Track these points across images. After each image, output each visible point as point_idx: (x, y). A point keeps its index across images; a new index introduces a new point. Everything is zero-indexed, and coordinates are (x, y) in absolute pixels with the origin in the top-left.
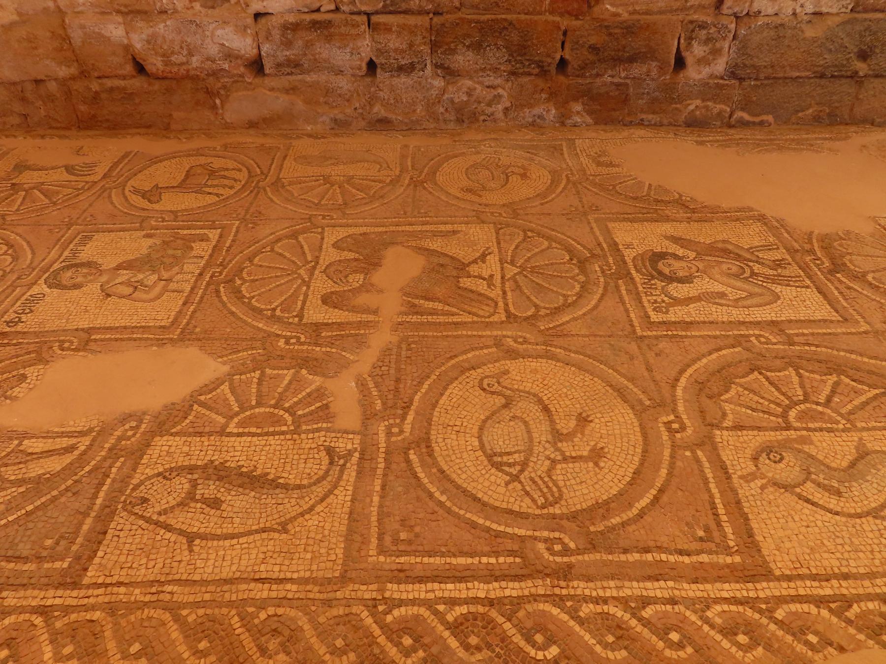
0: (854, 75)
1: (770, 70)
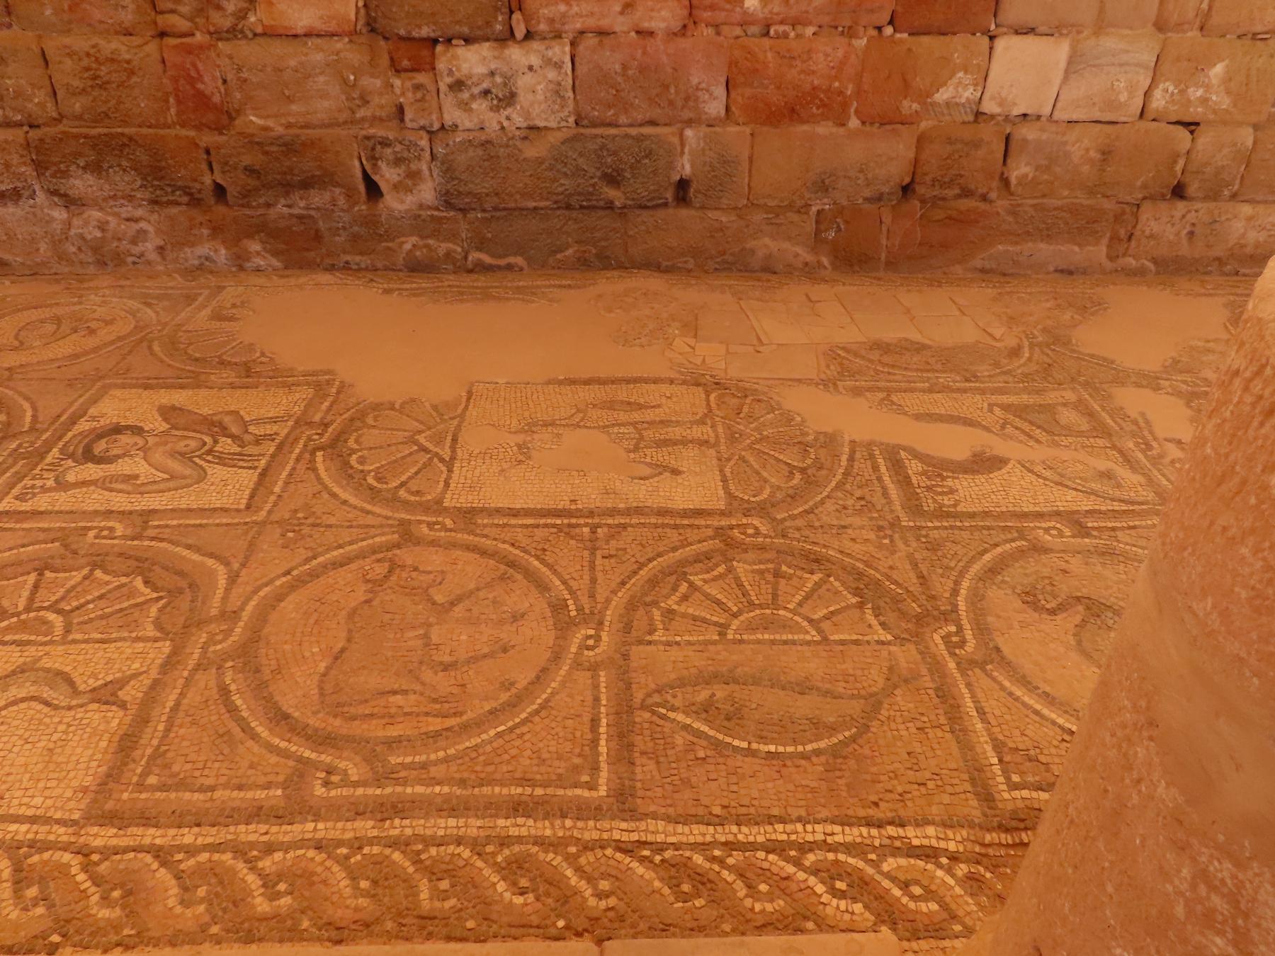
0: (610, 206)
1: (495, 199)
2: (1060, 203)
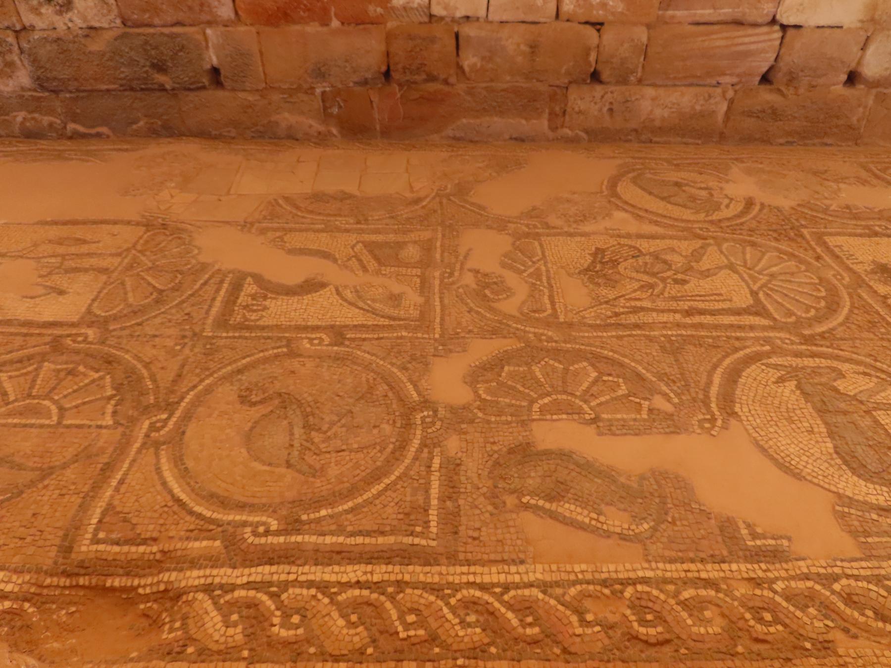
0: (162, 89)
1: (76, 83)
2: (505, 86)
